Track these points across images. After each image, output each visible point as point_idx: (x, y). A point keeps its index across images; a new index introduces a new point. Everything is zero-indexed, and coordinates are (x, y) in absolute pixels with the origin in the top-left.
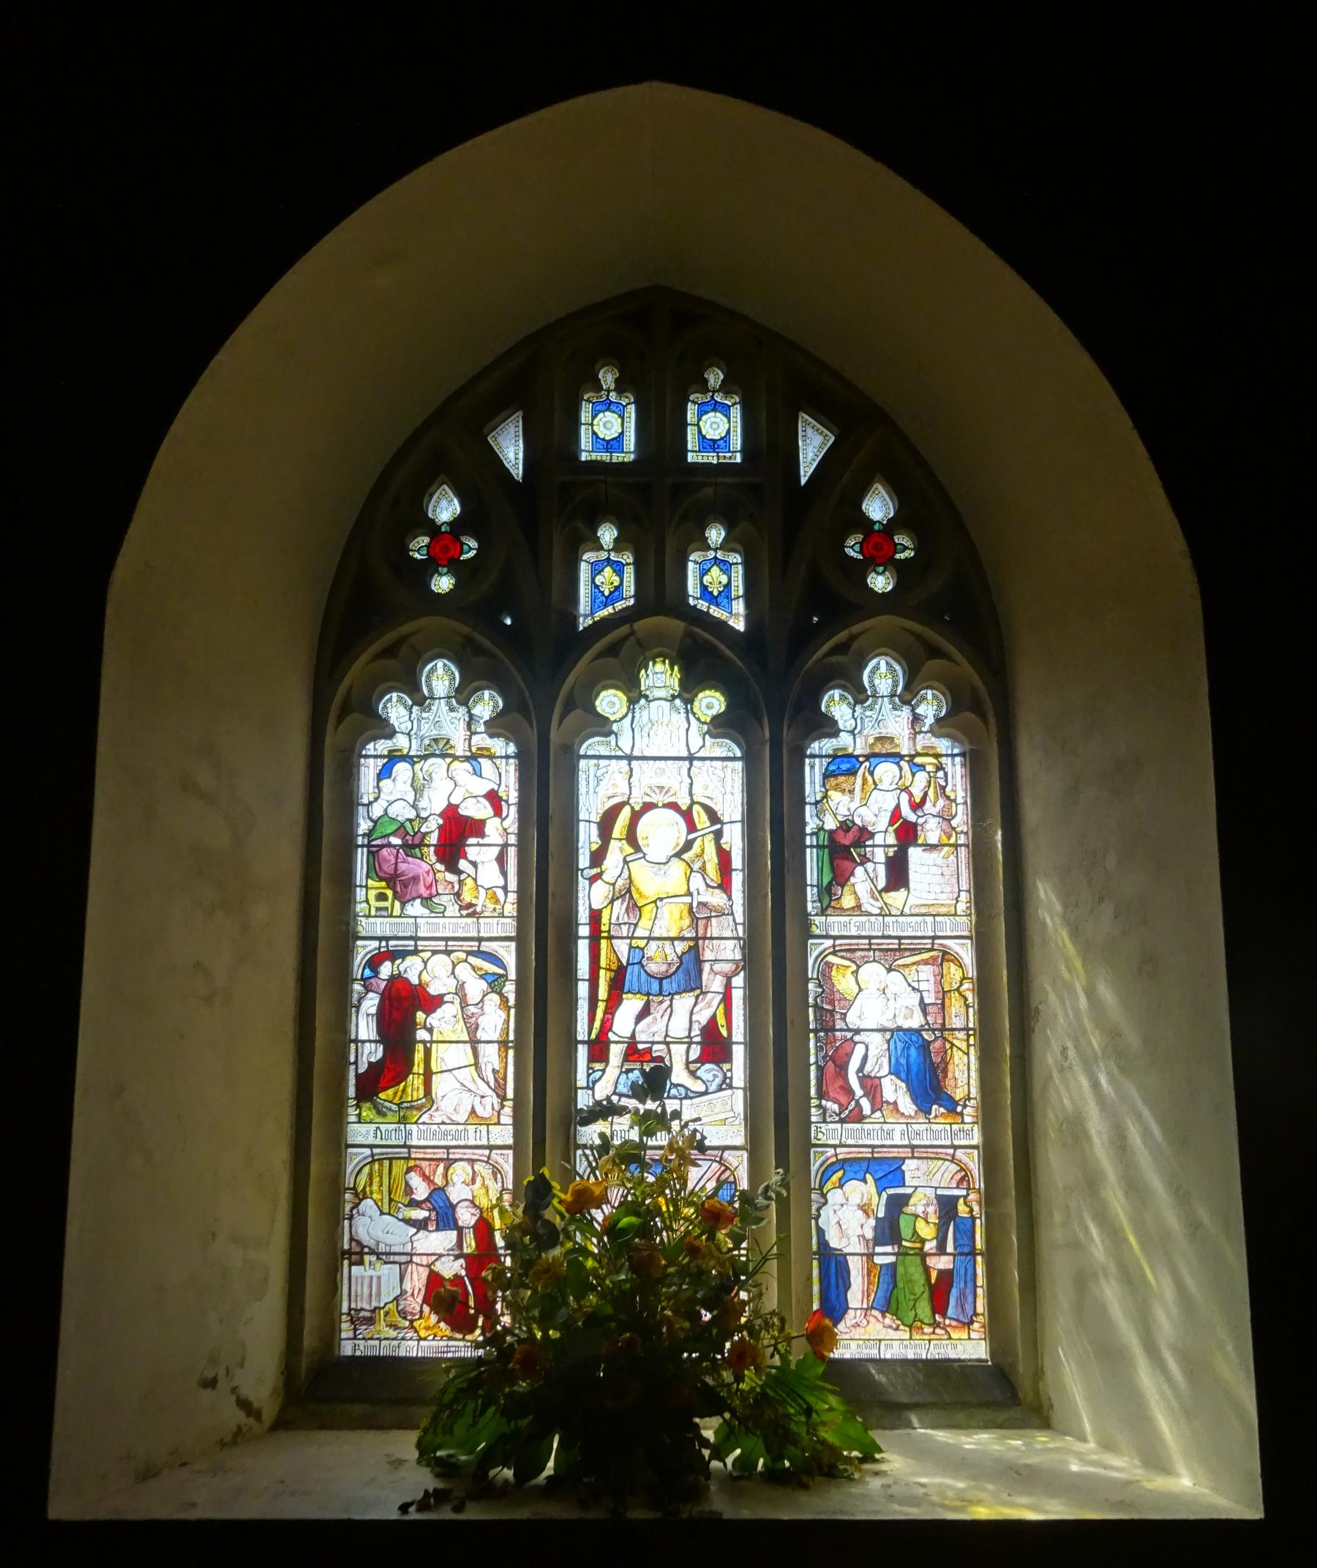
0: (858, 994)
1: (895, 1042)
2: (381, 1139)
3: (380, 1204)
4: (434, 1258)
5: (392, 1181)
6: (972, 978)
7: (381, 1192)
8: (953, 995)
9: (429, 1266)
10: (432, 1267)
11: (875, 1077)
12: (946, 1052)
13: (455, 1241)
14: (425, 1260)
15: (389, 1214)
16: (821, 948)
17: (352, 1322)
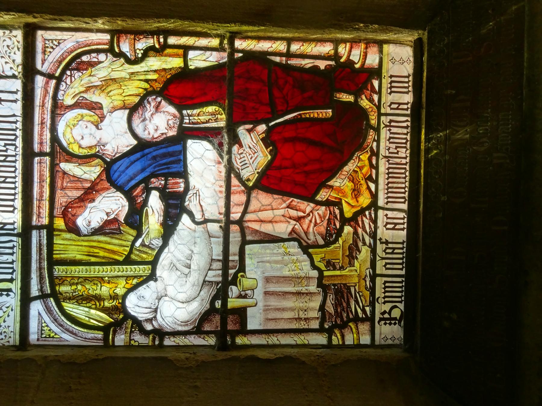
2: (11, 281)
3: (135, 281)
4: (234, 181)
5: (93, 259)
7: (112, 279)
9: (249, 191)
10: (251, 184)
13: (206, 144)
14: (238, 198)
15: (154, 263)
17: (343, 326)
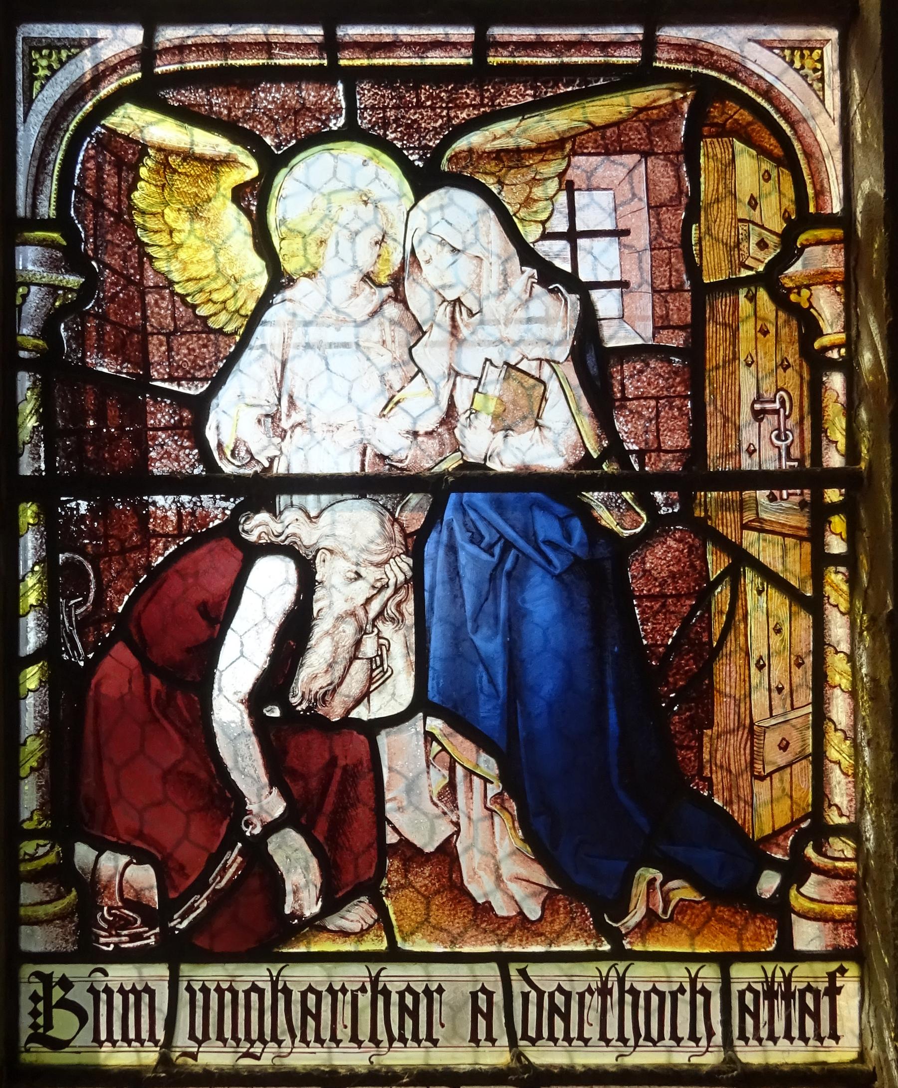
0: (264, 303)
1: (452, 549)
6: (846, 219)
8: (744, 305)
11: (347, 722)
12: (704, 596)
16: (85, 64)
